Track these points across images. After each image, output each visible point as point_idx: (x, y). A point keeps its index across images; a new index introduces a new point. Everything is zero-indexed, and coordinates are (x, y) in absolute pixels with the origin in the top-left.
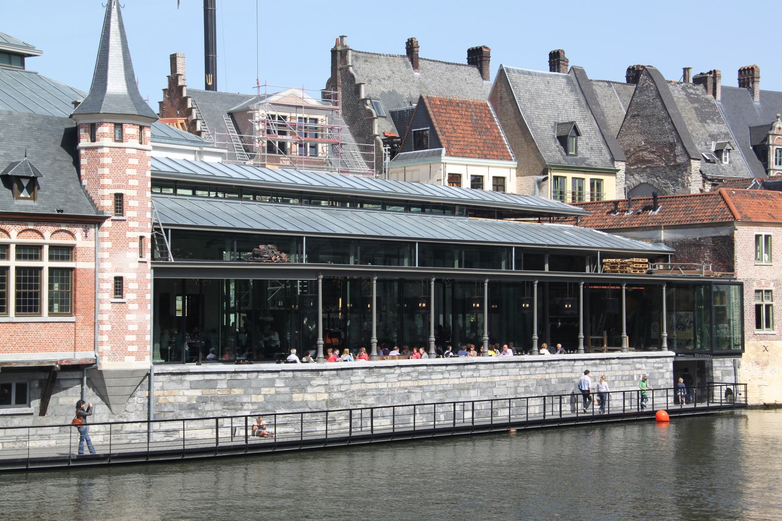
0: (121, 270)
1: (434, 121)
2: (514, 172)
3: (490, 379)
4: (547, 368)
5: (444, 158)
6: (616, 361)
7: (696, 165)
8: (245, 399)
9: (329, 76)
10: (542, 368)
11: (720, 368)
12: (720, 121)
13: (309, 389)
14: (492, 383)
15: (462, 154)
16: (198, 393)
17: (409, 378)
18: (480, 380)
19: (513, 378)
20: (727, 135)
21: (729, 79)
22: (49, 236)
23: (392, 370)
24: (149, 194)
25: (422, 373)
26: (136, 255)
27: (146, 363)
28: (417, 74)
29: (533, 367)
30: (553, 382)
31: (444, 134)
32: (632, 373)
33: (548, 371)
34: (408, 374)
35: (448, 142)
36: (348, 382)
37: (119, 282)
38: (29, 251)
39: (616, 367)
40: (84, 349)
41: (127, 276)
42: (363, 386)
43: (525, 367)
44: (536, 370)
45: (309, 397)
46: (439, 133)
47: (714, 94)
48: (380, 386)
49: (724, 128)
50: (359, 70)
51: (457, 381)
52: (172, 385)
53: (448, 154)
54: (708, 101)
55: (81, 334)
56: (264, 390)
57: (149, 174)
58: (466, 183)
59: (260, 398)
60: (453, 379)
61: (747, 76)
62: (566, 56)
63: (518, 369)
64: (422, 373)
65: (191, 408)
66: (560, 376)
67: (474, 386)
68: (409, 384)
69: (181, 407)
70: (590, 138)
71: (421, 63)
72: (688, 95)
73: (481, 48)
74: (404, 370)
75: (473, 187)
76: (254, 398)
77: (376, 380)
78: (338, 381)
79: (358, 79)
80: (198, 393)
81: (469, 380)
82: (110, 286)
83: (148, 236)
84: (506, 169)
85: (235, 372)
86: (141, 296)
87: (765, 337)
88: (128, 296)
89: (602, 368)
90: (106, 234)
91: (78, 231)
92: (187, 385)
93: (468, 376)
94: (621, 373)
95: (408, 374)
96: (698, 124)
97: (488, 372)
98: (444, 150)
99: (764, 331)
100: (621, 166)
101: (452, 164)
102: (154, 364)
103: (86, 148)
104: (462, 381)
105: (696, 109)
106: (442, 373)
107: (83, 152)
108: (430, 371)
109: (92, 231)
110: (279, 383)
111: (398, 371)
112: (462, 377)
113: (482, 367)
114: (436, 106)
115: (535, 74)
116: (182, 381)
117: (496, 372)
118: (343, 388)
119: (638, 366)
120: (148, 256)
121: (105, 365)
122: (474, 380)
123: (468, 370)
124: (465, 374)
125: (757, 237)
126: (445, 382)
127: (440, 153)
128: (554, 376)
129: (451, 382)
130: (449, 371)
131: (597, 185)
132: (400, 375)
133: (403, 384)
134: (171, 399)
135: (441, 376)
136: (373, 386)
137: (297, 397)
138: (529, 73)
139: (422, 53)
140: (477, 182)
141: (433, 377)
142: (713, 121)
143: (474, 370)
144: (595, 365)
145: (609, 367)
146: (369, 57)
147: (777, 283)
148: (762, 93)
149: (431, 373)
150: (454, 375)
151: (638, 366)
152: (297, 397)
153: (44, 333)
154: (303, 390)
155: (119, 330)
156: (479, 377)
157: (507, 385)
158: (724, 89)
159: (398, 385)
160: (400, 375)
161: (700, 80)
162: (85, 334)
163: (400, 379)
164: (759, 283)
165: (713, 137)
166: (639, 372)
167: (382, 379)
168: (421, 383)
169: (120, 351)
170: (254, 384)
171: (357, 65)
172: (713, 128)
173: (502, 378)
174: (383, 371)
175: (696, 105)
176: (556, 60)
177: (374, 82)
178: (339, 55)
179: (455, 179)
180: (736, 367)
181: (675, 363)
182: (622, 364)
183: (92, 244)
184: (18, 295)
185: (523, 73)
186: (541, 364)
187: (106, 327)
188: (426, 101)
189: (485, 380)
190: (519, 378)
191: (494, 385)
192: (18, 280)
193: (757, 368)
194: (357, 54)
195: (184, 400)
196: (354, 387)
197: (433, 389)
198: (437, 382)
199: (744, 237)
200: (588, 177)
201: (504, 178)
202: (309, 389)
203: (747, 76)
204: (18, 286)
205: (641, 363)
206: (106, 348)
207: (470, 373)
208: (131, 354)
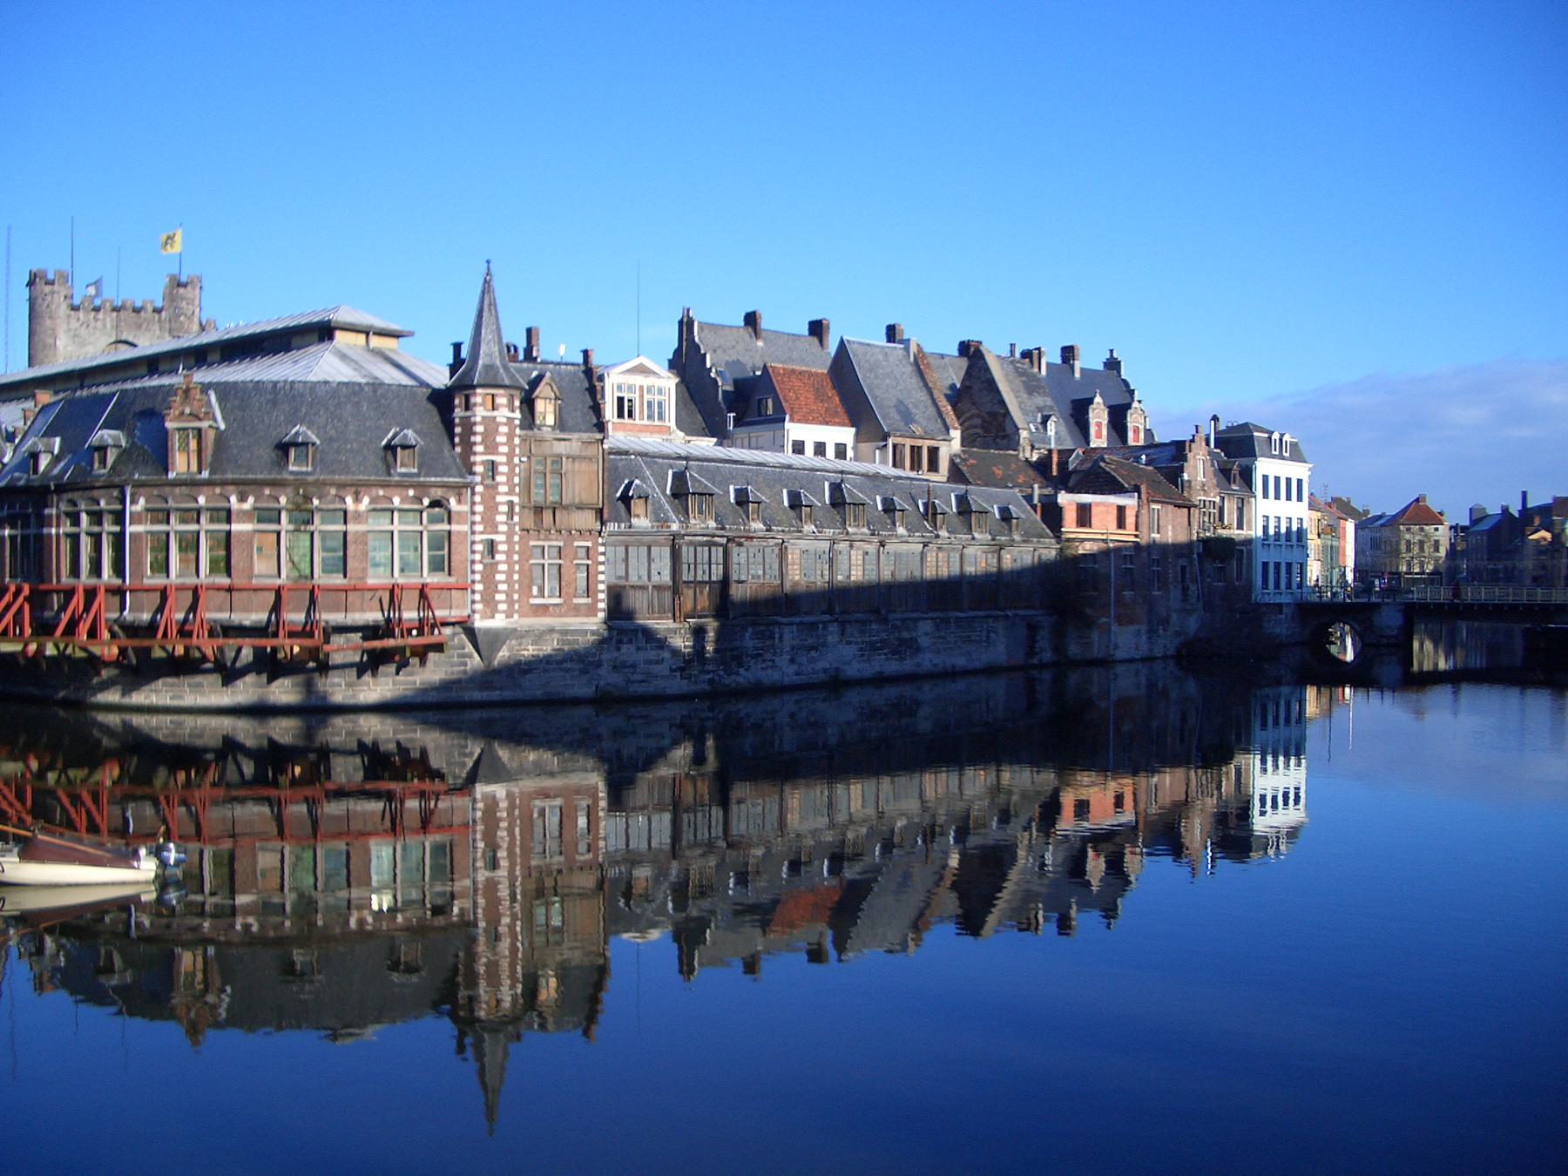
1: (777, 388)
5: (788, 425)
9: (676, 345)
12: (1045, 395)
15: (805, 420)
20: (1051, 408)
21: (1052, 356)
28: (760, 344)
31: (787, 401)
35: (792, 409)
46: (782, 400)
49: (1049, 402)
53: (792, 420)
54: (1034, 375)
58: (809, 449)
61: (1068, 353)
62: (902, 327)
70: (926, 407)
71: (763, 334)
72: (1016, 369)
73: (821, 321)
75: (816, 453)
84: (846, 435)
90: (477, 499)
98: (787, 418)
103: (461, 418)
105: (1023, 382)
107: (457, 421)
114: (779, 374)
115: (874, 346)
127: (784, 421)
138: (868, 345)
139: (765, 324)
140: (820, 449)
142: (1039, 394)
148: (1082, 370)
161: (1027, 354)
165: (1040, 409)
172: (1040, 400)
175: (1024, 379)
176: (892, 333)
177: (719, 351)
178: (686, 325)
179: (799, 448)
185: (862, 344)
188: (770, 371)
194: (702, 326)
203: (1068, 353)
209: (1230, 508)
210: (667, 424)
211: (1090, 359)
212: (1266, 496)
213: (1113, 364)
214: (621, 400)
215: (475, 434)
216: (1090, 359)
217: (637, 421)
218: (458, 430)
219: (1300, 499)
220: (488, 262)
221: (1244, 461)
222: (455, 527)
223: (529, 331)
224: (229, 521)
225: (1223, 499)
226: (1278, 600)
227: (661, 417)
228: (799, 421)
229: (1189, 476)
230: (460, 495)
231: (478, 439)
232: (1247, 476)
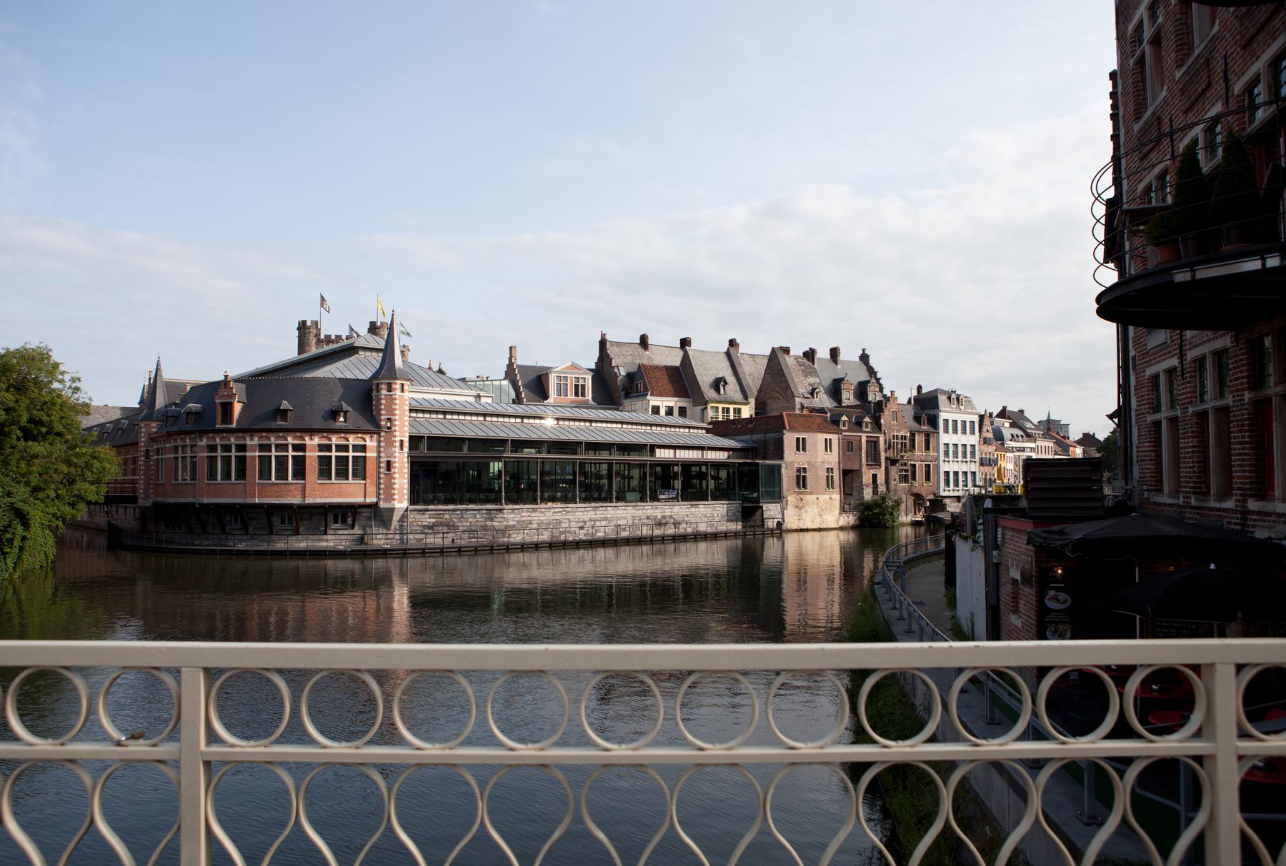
0: (389, 457)
2: (691, 404)
5: (648, 397)
7: (797, 400)
8: (459, 524)
11: (771, 511)
13: (495, 519)
15: (661, 394)
16: (434, 520)
21: (823, 354)
22: (353, 440)
24: (406, 418)
25: (569, 512)
26: (397, 449)
27: (405, 504)
30: (659, 517)
34: (560, 512)
37: (389, 464)
38: (341, 448)
40: (371, 497)
41: (392, 460)
42: (530, 518)
45: (495, 524)
47: (813, 363)
48: (541, 518)
50: (611, 351)
52: (421, 516)
53: (652, 395)
55: (368, 489)
56: (470, 520)
57: (407, 408)
58: (663, 412)
59: (468, 524)
60: (591, 515)
61: (834, 353)
64: (569, 512)
65: (431, 527)
67: (605, 519)
69: (424, 527)
72: (798, 362)
74: (556, 510)
76: (465, 524)
78: (512, 516)
79: (612, 356)
80: (434, 520)
82: (383, 465)
83: (406, 440)
85: (454, 510)
86: (401, 470)
87: (802, 493)
88: (393, 470)
89: (693, 510)
91: (367, 437)
92: (427, 516)
93: (600, 513)
96: (802, 378)
99: (802, 490)
100: (752, 401)
101: (654, 401)
102: (411, 504)
104: (597, 516)
109: (375, 436)
110: (478, 516)
111: (552, 510)
113: (609, 508)
116: (424, 514)
117: (618, 512)
118: (516, 519)
120: (406, 449)
121: (382, 505)
125: (798, 439)
131: (739, 411)
133: (556, 518)
134: (420, 523)
137: (488, 523)
142: (812, 376)
146: (618, 344)
147: (809, 463)
150: (590, 513)
152: (488, 523)
153: (350, 489)
154: (492, 519)
155: (390, 487)
158: (819, 359)
162: (371, 489)
164: (798, 464)
165: (810, 385)
168: (569, 517)
169: (390, 497)
170: (464, 516)
171: (611, 348)
172: (812, 380)
174: (543, 510)
178: (603, 343)
179: (656, 410)
180: (783, 509)
181: (743, 508)
183: (375, 444)
184: (336, 470)
187: (382, 486)
192: (336, 462)
193: (797, 510)
194: (613, 343)
195: (426, 524)
196: (523, 519)
199: (789, 438)
200: (732, 407)
201: (659, 407)
202: (495, 519)
203: (834, 353)
204: (336, 465)
206: (382, 497)
208: (394, 500)
209: (919, 439)
210: (586, 398)
211: (850, 355)
212: (946, 431)
213: (864, 358)
214: (577, 386)
215: (381, 404)
216: (850, 355)
217: (569, 397)
218: (374, 403)
219: (973, 432)
221: (931, 412)
222: (368, 454)
223: (511, 348)
224: (365, 452)
225: (913, 435)
226: (956, 494)
227: (583, 395)
228: (657, 395)
229: (885, 421)
230: (371, 437)
231: (383, 407)
232: (933, 422)
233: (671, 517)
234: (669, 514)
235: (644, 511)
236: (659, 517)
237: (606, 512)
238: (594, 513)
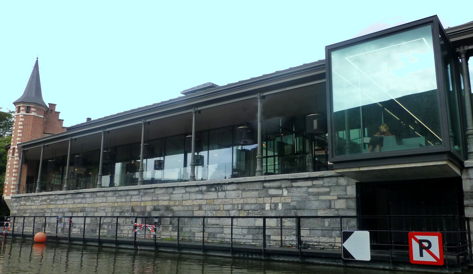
3: (93, 205)
4: (142, 196)
6: (234, 187)
10: (137, 197)
14: (94, 208)
17: (45, 203)
18: (86, 205)
19: (110, 204)
23: (38, 199)
29: (128, 195)
30: (148, 209)
32: (261, 200)
33: (143, 199)
34: (45, 201)
36: (19, 205)
39: (233, 194)
43: (121, 196)
44: (131, 198)
51: (71, 206)
63: (115, 198)
64: (52, 200)
66: (155, 204)
68: (45, 207)
77: (30, 204)
78: (16, 204)
81: (79, 206)
89: (212, 195)
94: (241, 201)
95: (45, 201)
97: (92, 199)
104: (75, 206)
106: (63, 200)
108: (56, 198)
112: (74, 203)
113: (88, 195)
117: (97, 200)
118: (18, 208)
119: (272, 192)
122: (82, 205)
123: (78, 198)
124: (76, 201)
126: (64, 206)
128: (150, 203)
129: (67, 206)
130: (67, 199)
132: (42, 201)
135: (62, 202)
136: (29, 207)
141: (58, 203)
143: (83, 198)
144: (201, 192)
145: (221, 194)
149: (56, 200)
151: (272, 192)
156: (86, 203)
157: (106, 211)
159: (40, 207)
160: (42, 201)
163: (41, 203)
166: (275, 200)
167: (33, 204)
168: (51, 206)
173: (102, 205)
174: (34, 198)
182: (244, 190)
186: (136, 193)
189: (90, 206)
190: (116, 205)
191: (95, 210)
197: (57, 210)
198: (59, 206)
205: (280, 188)
207: (79, 200)
220: (37, 58)
233: (168, 208)
234: (166, 203)
235: (128, 198)
236: (148, 209)
237: (84, 201)
238: (70, 201)
